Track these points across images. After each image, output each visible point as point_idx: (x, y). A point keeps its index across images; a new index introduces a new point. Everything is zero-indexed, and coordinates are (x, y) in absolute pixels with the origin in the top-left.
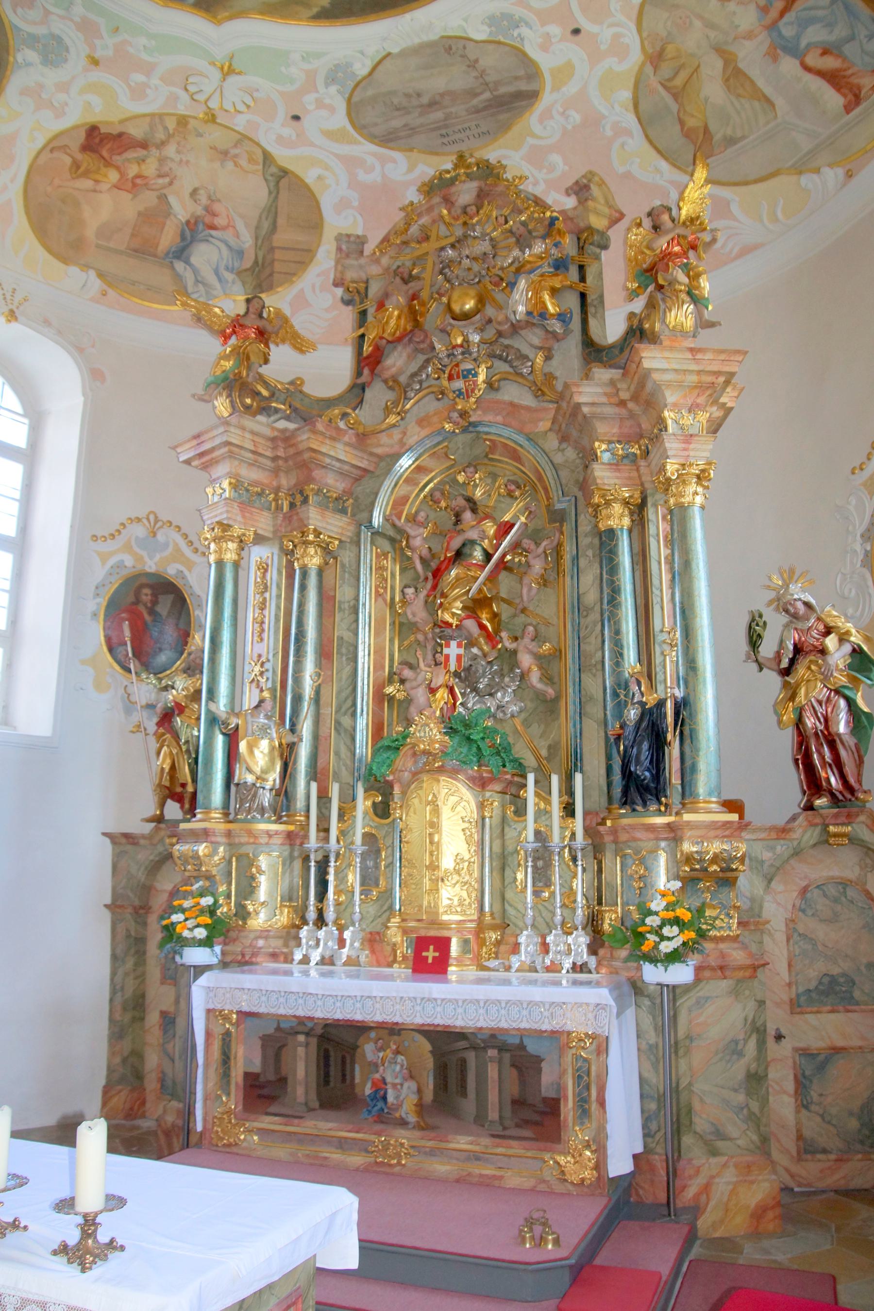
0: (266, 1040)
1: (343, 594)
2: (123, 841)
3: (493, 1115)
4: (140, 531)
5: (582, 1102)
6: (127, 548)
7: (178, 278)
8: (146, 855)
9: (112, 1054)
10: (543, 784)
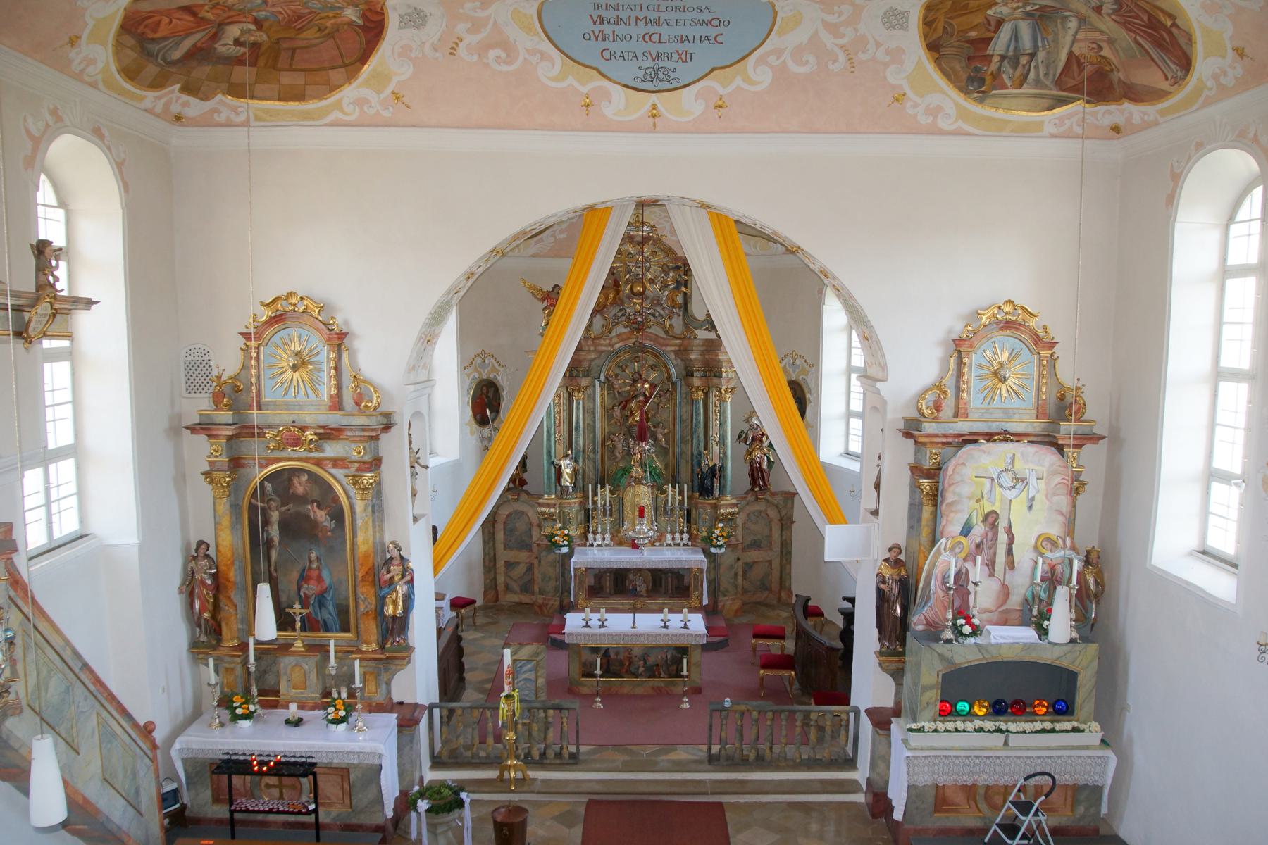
0: (595, 576)
4: (479, 361)
5: (696, 587)
6: (476, 370)
10: (673, 487)
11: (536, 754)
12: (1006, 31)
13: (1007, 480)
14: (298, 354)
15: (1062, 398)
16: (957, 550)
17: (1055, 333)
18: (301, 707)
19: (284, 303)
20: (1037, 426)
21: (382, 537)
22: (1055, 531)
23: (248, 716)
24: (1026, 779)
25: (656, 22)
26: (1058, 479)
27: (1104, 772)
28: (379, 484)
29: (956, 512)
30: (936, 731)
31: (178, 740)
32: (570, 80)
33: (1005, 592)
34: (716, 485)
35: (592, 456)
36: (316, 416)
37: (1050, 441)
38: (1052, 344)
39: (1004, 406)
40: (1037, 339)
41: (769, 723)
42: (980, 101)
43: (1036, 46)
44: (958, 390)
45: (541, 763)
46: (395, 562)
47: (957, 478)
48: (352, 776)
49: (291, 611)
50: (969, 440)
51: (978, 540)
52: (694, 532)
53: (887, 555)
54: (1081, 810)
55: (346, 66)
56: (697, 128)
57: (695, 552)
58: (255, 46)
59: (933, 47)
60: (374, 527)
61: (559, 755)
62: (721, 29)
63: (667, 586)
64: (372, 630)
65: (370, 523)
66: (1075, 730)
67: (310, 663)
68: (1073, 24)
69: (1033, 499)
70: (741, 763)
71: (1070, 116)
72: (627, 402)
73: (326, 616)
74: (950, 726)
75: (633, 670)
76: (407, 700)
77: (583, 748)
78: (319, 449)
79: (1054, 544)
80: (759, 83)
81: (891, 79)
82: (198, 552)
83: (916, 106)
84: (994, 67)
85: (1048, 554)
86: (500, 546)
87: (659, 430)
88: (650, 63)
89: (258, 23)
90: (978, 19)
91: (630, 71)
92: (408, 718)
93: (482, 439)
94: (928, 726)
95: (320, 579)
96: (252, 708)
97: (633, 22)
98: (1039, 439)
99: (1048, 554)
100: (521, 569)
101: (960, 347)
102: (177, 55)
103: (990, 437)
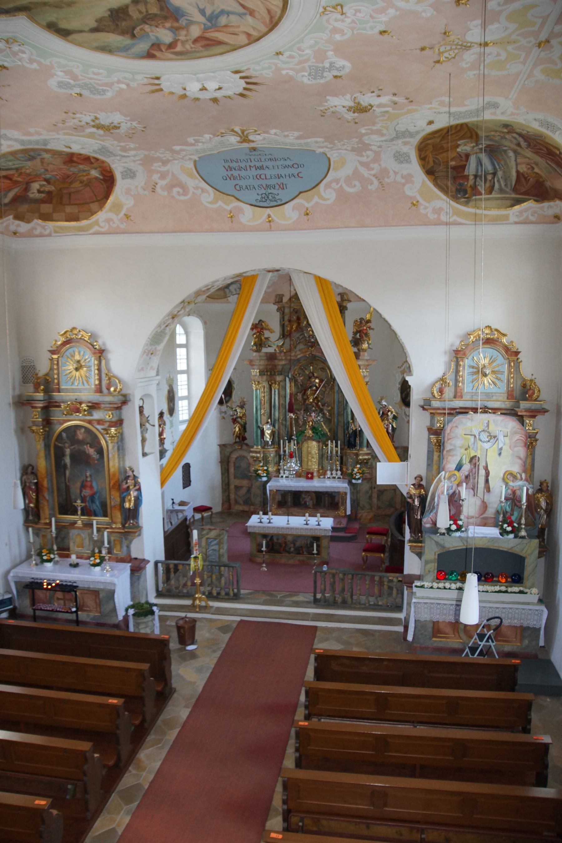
1: (282, 393)
2: (222, 447)
3: (327, 505)
7: (225, 293)
8: (229, 450)
9: (223, 496)
11: (215, 593)
12: (473, 160)
13: (484, 436)
14: (79, 362)
15: (524, 386)
16: (453, 479)
17: (518, 345)
18: (78, 558)
19: (71, 333)
20: (508, 404)
21: (124, 464)
22: (516, 468)
23: (50, 561)
24: (488, 620)
25: (262, 168)
26: (517, 437)
27: (541, 620)
28: (122, 434)
29: (453, 456)
30: (432, 588)
31: (13, 571)
32: (220, 203)
33: (484, 506)
34: (358, 442)
35: (284, 423)
36: (87, 394)
37: (511, 412)
38: (517, 353)
39: (486, 391)
40: (507, 349)
41: (349, 581)
42: (466, 204)
43: (495, 168)
44: (457, 381)
45: (217, 598)
46: (130, 478)
47: (453, 435)
48: (101, 596)
49: (76, 504)
50: (464, 411)
51: (467, 473)
52: (344, 470)
53: (414, 482)
54: (526, 642)
55: (98, 201)
56: (295, 227)
57: (343, 482)
58: (49, 193)
59: (430, 172)
60: (119, 458)
61: (227, 594)
62: (300, 169)
63: (324, 502)
64: (118, 516)
65: (116, 456)
66: (521, 592)
67: (84, 534)
68: (511, 154)
69: (501, 449)
70: (333, 604)
71: (526, 210)
72: (306, 390)
73: (95, 508)
74: (441, 585)
75: (287, 549)
76: (140, 557)
77: (242, 592)
78: (90, 414)
79: (515, 477)
80: (329, 199)
81: (408, 192)
82: (28, 470)
83: (426, 208)
84: (471, 182)
85: (511, 484)
86: (232, 476)
87: (325, 408)
88: (263, 191)
89: (48, 181)
90: (451, 155)
91: (253, 196)
92: (137, 567)
93: (221, 412)
94: (426, 584)
95: (91, 487)
96: (52, 556)
97: (248, 169)
98: (508, 412)
99: (511, 484)
100: (244, 490)
101: (458, 355)
102: (6, 200)
103: (475, 410)
